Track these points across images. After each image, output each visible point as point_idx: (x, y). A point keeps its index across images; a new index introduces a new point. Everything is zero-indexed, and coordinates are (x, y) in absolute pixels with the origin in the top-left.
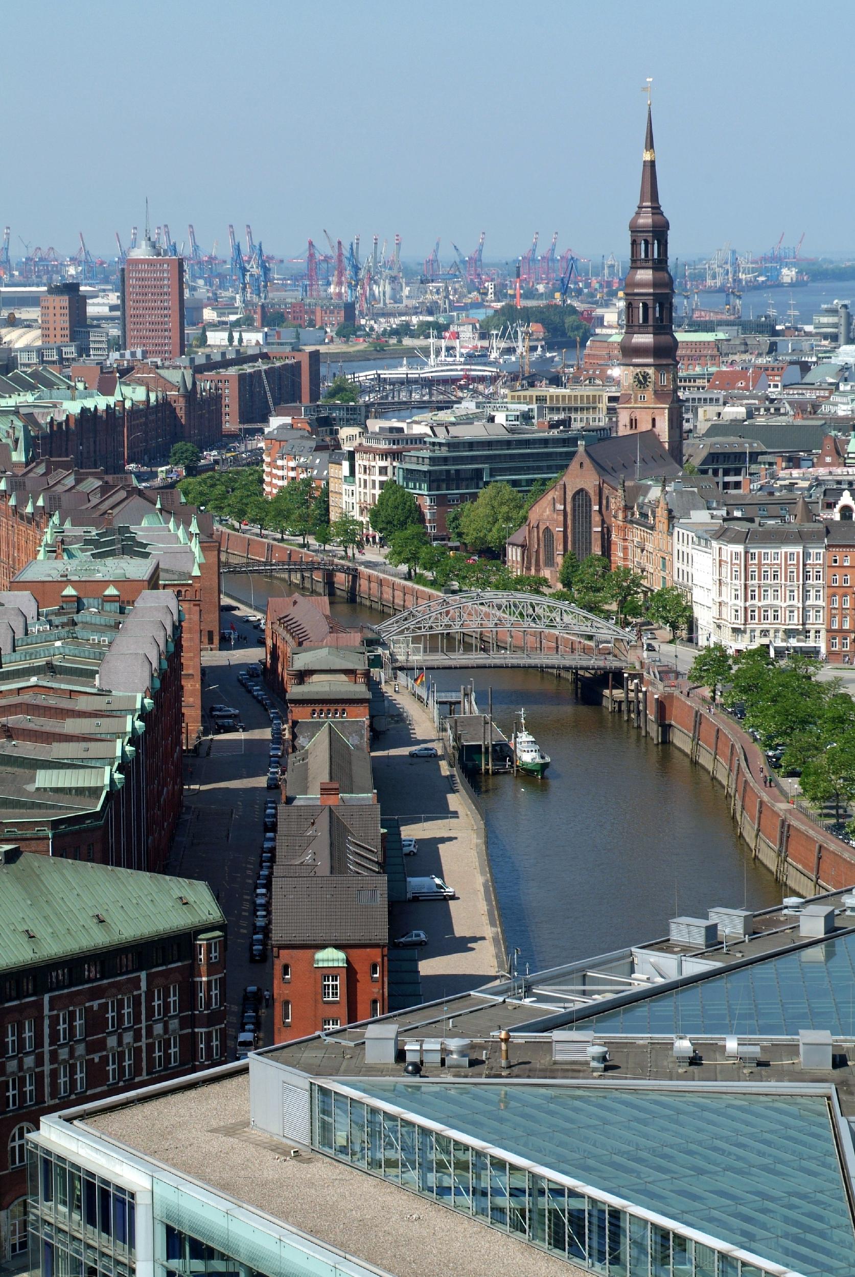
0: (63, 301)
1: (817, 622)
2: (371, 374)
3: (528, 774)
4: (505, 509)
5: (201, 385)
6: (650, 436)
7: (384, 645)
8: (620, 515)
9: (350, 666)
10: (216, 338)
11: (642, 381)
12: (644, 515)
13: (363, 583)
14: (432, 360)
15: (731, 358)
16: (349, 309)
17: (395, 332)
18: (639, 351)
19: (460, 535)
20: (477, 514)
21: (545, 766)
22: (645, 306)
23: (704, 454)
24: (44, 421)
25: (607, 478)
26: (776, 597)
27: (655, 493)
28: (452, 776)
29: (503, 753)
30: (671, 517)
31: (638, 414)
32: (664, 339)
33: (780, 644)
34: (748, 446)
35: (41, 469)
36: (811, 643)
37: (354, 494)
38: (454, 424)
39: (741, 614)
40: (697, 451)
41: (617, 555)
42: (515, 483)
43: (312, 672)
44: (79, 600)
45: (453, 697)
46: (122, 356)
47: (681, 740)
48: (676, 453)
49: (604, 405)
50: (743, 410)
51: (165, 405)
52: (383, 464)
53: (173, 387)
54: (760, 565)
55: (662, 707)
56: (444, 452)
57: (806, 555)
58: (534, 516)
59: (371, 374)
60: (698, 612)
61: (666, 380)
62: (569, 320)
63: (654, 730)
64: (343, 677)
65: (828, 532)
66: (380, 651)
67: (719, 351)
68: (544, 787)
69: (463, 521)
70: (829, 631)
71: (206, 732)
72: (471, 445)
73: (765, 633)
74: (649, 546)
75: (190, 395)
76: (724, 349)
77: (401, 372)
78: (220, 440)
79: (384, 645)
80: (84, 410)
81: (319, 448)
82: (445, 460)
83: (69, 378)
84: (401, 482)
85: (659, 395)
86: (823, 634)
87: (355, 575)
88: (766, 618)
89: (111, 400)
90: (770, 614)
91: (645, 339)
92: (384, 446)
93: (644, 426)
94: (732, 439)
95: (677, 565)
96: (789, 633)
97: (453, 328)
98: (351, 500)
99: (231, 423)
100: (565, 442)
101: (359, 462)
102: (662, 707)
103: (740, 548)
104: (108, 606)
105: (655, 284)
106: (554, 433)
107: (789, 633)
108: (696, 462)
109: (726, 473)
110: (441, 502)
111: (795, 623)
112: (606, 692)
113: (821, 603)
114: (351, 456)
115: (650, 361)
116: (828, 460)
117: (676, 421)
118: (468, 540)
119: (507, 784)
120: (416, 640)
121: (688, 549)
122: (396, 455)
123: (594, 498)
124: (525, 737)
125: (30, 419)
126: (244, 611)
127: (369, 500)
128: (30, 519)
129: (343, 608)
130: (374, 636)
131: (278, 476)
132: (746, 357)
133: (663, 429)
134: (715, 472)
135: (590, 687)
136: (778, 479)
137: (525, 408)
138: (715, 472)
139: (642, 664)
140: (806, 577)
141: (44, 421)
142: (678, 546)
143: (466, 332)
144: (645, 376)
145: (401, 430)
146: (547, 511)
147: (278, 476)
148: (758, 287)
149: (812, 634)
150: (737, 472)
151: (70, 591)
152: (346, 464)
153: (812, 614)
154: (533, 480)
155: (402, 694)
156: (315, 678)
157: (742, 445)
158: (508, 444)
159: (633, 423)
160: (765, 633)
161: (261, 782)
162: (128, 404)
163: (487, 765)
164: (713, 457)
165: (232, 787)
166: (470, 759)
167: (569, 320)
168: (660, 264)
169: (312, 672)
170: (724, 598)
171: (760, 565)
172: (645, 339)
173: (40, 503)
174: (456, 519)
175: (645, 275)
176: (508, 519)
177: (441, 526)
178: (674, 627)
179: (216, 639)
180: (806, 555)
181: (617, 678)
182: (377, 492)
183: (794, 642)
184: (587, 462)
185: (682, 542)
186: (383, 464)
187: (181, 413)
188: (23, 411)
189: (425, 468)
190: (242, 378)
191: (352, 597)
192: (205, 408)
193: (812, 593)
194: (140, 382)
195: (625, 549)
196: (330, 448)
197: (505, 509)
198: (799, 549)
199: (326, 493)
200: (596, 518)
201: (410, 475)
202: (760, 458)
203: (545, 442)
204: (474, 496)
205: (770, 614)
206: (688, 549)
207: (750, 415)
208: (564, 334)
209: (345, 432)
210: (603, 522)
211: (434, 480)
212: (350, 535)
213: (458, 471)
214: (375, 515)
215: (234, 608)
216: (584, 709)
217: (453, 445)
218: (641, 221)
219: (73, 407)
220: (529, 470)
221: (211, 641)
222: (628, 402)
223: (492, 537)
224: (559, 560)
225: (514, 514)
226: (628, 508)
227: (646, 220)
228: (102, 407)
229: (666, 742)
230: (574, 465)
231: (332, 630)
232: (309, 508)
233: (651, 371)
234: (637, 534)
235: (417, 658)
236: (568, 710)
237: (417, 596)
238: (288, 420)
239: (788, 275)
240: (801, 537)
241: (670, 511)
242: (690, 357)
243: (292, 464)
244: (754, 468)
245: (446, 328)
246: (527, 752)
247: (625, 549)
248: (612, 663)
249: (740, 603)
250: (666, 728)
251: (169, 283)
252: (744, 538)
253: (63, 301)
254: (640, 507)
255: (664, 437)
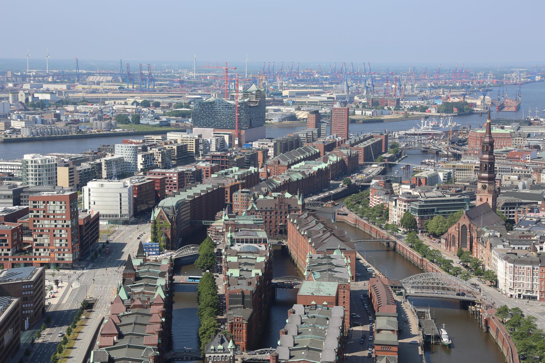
0: (314, 116)
1: (537, 288)
2: (403, 132)
3: (444, 346)
4: (441, 223)
5: (353, 153)
6: (486, 204)
7: (402, 288)
8: (476, 239)
9: (393, 329)
10: (358, 112)
11: (484, 187)
12: (483, 242)
13: (398, 246)
14: (422, 128)
15: (515, 138)
16: (398, 101)
17: (411, 109)
18: (483, 178)
19: (427, 229)
20: (433, 224)
21: (449, 345)
22: (486, 165)
23: (503, 203)
24: (307, 173)
25: (472, 221)
26: (523, 280)
27: (487, 235)
28: (422, 355)
29: (438, 337)
30: (491, 246)
31: (482, 197)
32: (492, 175)
33: (524, 294)
34: (517, 200)
35: (306, 215)
36: (534, 295)
37: (396, 214)
38: (426, 192)
39: (512, 284)
40: (502, 200)
41: (474, 250)
42: (444, 213)
43: (382, 330)
44: (316, 305)
45: (423, 310)
46: (330, 138)
47: (492, 333)
48: (495, 207)
49: (474, 168)
50: (517, 177)
51: (342, 161)
52: (405, 204)
53: (345, 155)
54: (518, 270)
55: (487, 321)
56: (423, 204)
57: (534, 269)
58: (450, 230)
59: (403, 132)
60: (498, 278)
61: (492, 187)
62: (465, 107)
63: (484, 328)
64: (390, 332)
65: (540, 261)
66: (403, 291)
67: (511, 136)
68: (449, 352)
69: (428, 225)
70: (540, 292)
71: (350, 328)
72: (431, 201)
73: (520, 290)
74: (484, 252)
75: (350, 158)
76: (513, 135)
77: (412, 131)
78: (358, 169)
79: (402, 288)
80: (319, 169)
81: (386, 194)
82: (423, 206)
83: (314, 147)
84: (410, 211)
85: (489, 192)
86: (538, 292)
87: (395, 243)
88: (520, 286)
89: (326, 165)
90: (522, 285)
91: (486, 175)
92: (405, 199)
93: (484, 201)
94: (513, 198)
95: (493, 261)
96: (527, 291)
97: (429, 109)
98: (395, 213)
99: (361, 162)
100: (460, 200)
101: (397, 203)
102: (487, 321)
103: (512, 265)
104: (324, 308)
105: (489, 159)
106: (456, 197)
107: (527, 291)
108: (500, 205)
109: (510, 209)
110: (422, 218)
111: (529, 288)
112: (470, 307)
113: (538, 283)
114: (396, 200)
115: (487, 182)
116: (543, 209)
117: (494, 200)
118: (430, 231)
119: (439, 348)
120: (412, 287)
121: (496, 258)
122: (408, 202)
123: (468, 228)
124: (444, 333)
125: (303, 173)
126: (363, 261)
127: (400, 214)
128: (303, 235)
129: (391, 253)
130: (400, 286)
131: (375, 201)
132: (520, 138)
133: (490, 202)
134: (507, 209)
135: (465, 305)
136: (526, 217)
137: (449, 171)
138: (507, 209)
139: (481, 300)
140: (533, 275)
141: (307, 173)
142: (493, 256)
143: (434, 112)
144: (485, 186)
145: (410, 193)
146: (453, 230)
147: (375, 201)
148: (528, 83)
149: (535, 292)
150: (514, 208)
151: (313, 303)
152: (394, 202)
153: (535, 286)
154: (450, 212)
155: (408, 308)
156: (382, 331)
157: (515, 200)
158: (443, 201)
159: (481, 200)
160: (520, 290)
161: (365, 353)
162: (331, 163)
163: (433, 342)
164: (506, 204)
165: (358, 355)
166: (428, 339)
167: (465, 107)
168: (491, 153)
169: (382, 330)
170: (507, 278)
171: (518, 270)
172: (486, 175)
173: (306, 233)
174: (426, 224)
175: (486, 156)
176: (442, 226)
177: (422, 225)
178: (491, 282)
179: (354, 279)
180: (534, 269)
181: (473, 303)
182: (403, 212)
183: (529, 294)
184: (466, 217)
185: (494, 254)
186: (405, 204)
187: (346, 163)
188: (302, 170)
189: (418, 208)
190: (365, 148)
191: (394, 249)
192: (353, 159)
193: (535, 280)
194: (335, 154)
195: (477, 249)
196: (391, 193)
197: (441, 223)
198: (531, 267)
199: (388, 209)
200: (468, 233)
201: (413, 210)
202: (521, 206)
203: (454, 200)
204: (432, 217)
205: (522, 285)
206: (496, 258)
207: (519, 179)
208: (463, 111)
209: (394, 185)
210: (471, 235)
211: (420, 212)
212: (395, 228)
213: (427, 211)
214: (402, 221)
215: (360, 259)
216: (463, 311)
217: (425, 202)
218: (486, 140)
219: (315, 169)
220: (448, 209)
221: (353, 279)
222: (480, 193)
223: (437, 232)
224: (457, 245)
225: (443, 225)
226: (478, 238)
227: (487, 140)
228: (324, 167)
229: (488, 332)
230: (462, 218)
231: (388, 304)
232: (383, 213)
233: (487, 185)
234: (480, 247)
235: (412, 292)
236: (458, 311)
237: (413, 255)
238: (377, 181)
239: (538, 78)
240: (532, 263)
241: (491, 244)
242: (502, 138)
243: (378, 198)
244: (519, 209)
245: (427, 108)
246: (445, 340)
247: (477, 249)
248: (472, 299)
249: (512, 281)
250: (488, 328)
251: (345, 113)
252: (513, 262)
253: (314, 116)
254: (482, 239)
255: (491, 204)
